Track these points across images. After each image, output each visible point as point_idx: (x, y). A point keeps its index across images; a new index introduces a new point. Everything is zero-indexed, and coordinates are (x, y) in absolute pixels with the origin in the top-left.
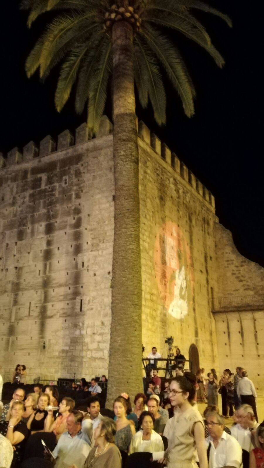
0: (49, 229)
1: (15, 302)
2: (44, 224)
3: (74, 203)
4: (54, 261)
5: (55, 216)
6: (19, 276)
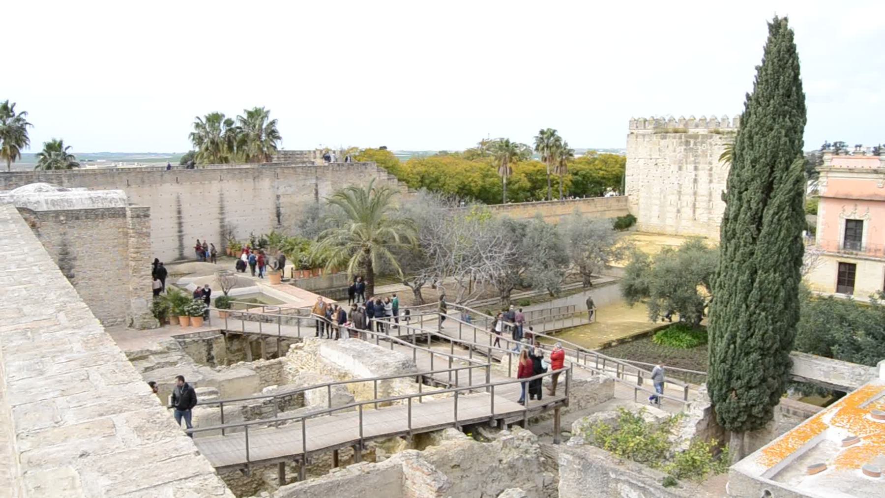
0: (696, 169)
1: (679, 199)
2: (693, 165)
3: (709, 159)
4: (699, 184)
5: (699, 163)
6: (680, 188)
